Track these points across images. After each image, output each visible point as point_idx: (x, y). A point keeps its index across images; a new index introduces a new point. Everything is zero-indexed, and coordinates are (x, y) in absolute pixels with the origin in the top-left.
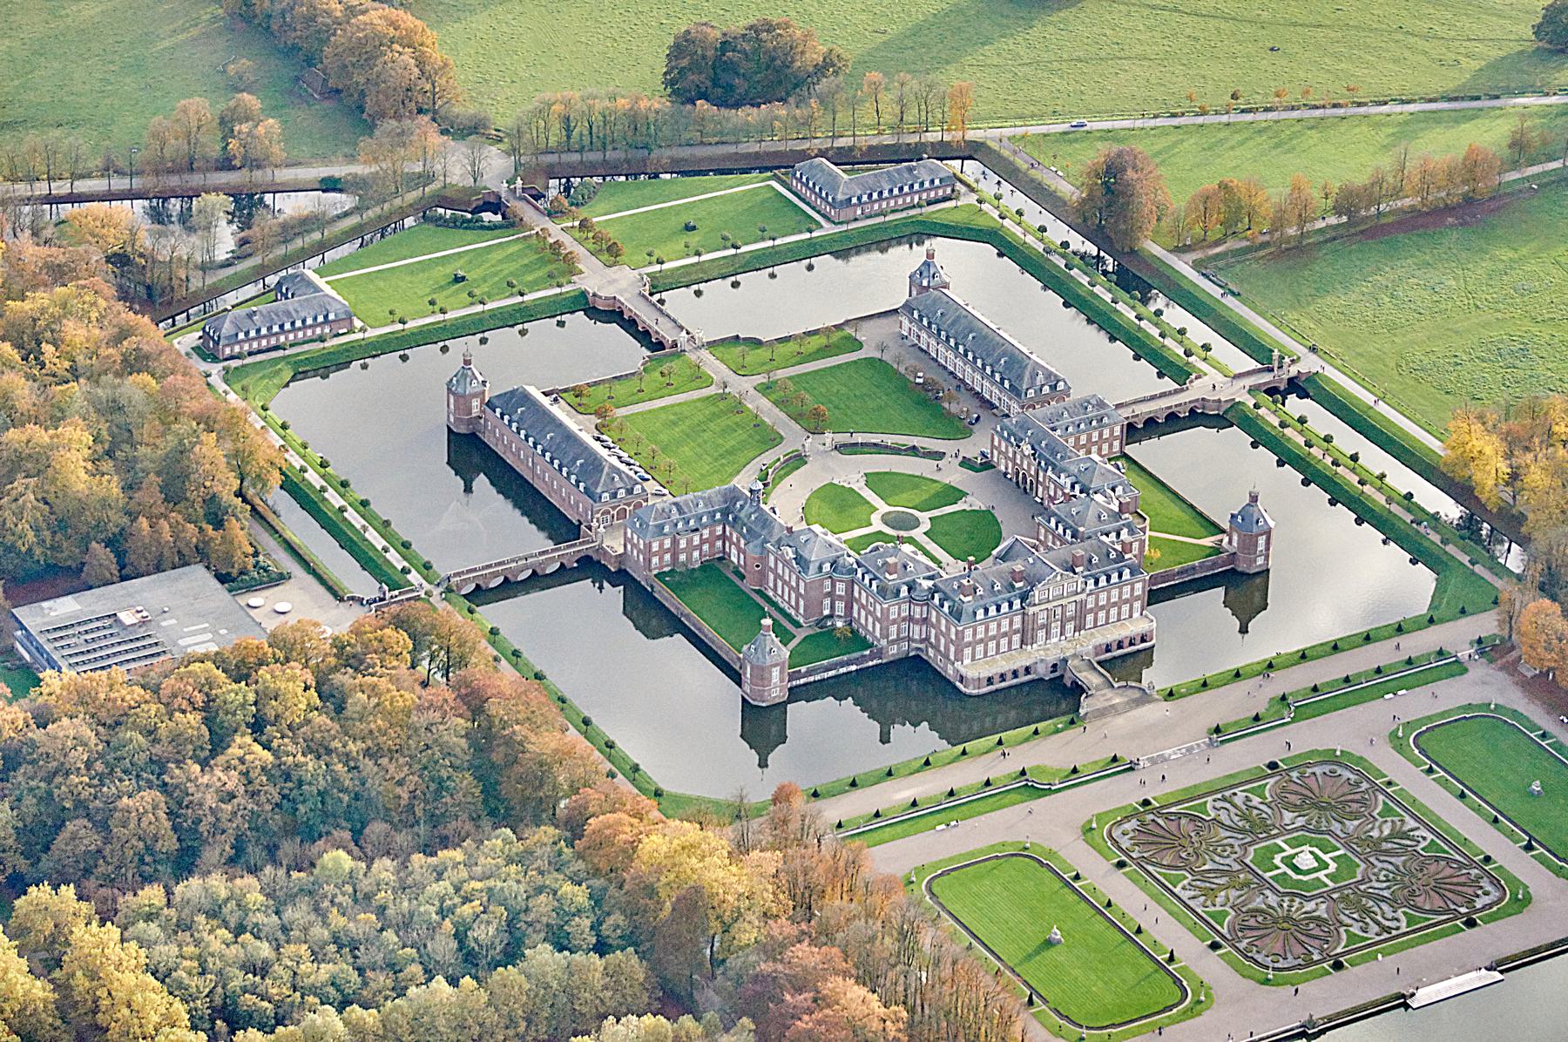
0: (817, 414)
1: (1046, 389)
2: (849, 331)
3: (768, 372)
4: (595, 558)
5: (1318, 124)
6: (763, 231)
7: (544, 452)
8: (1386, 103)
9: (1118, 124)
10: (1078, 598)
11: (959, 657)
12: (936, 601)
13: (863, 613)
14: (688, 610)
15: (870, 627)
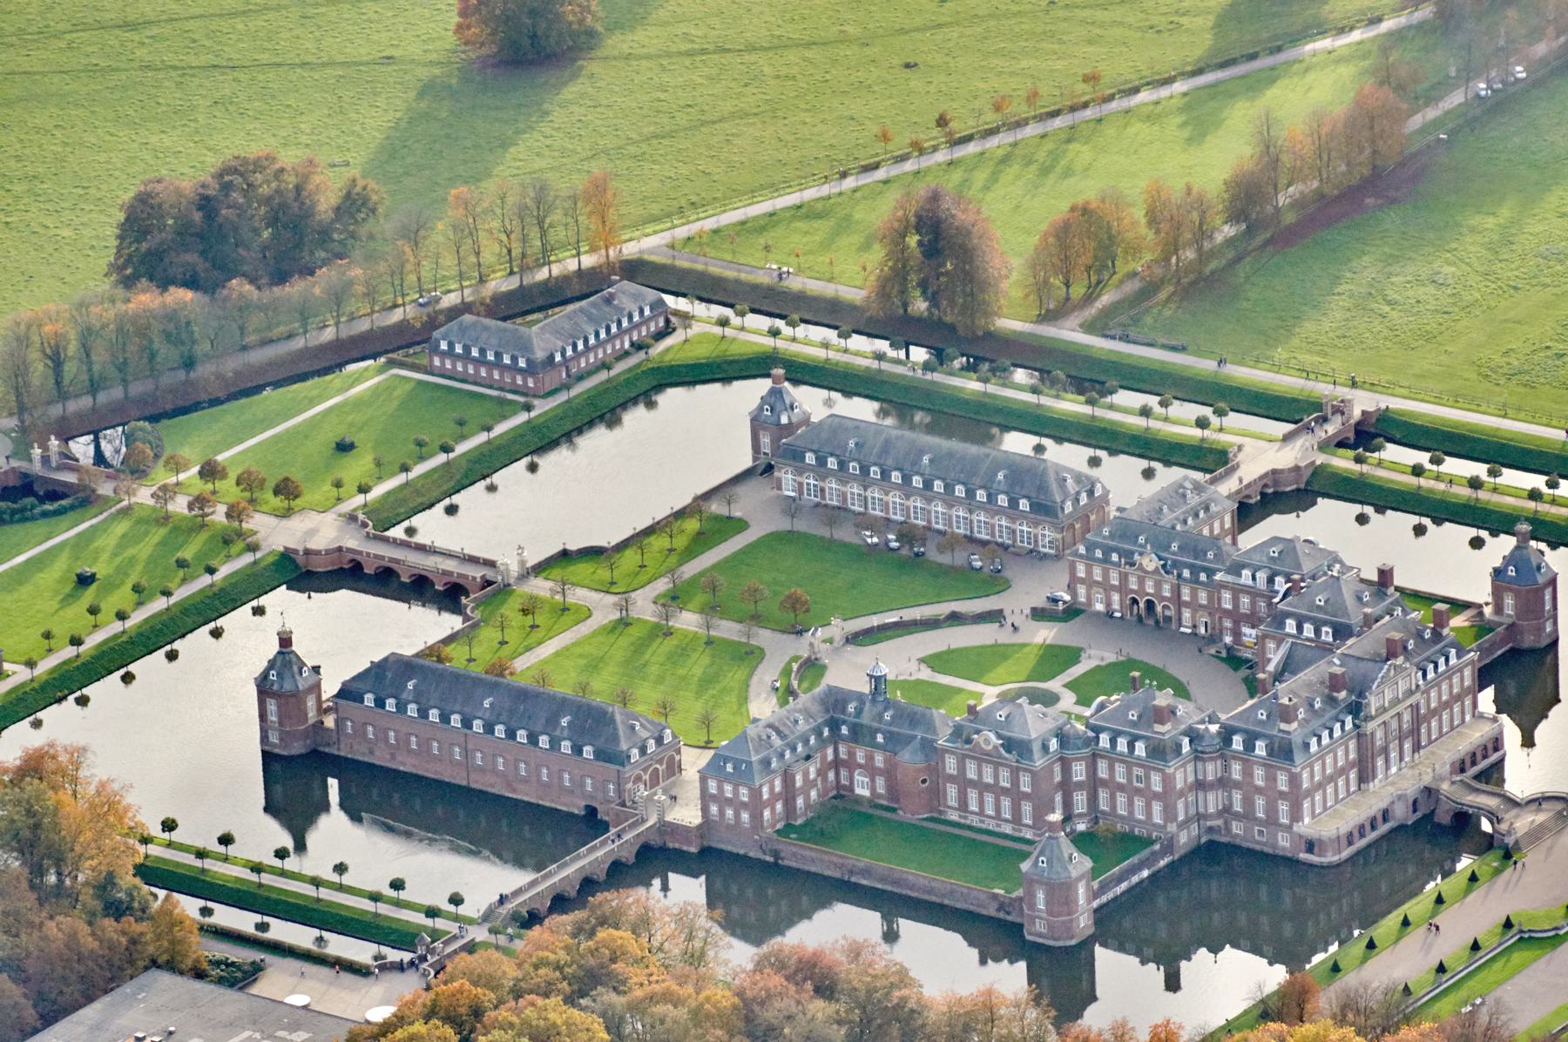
0: (794, 604)
1: (1084, 499)
2: (716, 507)
3: (672, 571)
4: (656, 841)
5: (1072, 134)
6: (461, 423)
7: (489, 729)
8: (1136, 90)
9: (810, 194)
10: (1412, 700)
11: (1296, 816)
12: (1237, 743)
13: (1121, 799)
14: (863, 862)
15: (1146, 814)
